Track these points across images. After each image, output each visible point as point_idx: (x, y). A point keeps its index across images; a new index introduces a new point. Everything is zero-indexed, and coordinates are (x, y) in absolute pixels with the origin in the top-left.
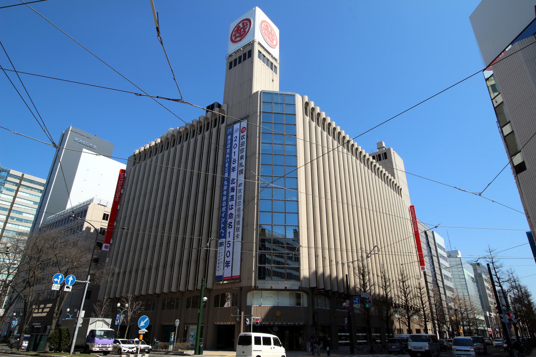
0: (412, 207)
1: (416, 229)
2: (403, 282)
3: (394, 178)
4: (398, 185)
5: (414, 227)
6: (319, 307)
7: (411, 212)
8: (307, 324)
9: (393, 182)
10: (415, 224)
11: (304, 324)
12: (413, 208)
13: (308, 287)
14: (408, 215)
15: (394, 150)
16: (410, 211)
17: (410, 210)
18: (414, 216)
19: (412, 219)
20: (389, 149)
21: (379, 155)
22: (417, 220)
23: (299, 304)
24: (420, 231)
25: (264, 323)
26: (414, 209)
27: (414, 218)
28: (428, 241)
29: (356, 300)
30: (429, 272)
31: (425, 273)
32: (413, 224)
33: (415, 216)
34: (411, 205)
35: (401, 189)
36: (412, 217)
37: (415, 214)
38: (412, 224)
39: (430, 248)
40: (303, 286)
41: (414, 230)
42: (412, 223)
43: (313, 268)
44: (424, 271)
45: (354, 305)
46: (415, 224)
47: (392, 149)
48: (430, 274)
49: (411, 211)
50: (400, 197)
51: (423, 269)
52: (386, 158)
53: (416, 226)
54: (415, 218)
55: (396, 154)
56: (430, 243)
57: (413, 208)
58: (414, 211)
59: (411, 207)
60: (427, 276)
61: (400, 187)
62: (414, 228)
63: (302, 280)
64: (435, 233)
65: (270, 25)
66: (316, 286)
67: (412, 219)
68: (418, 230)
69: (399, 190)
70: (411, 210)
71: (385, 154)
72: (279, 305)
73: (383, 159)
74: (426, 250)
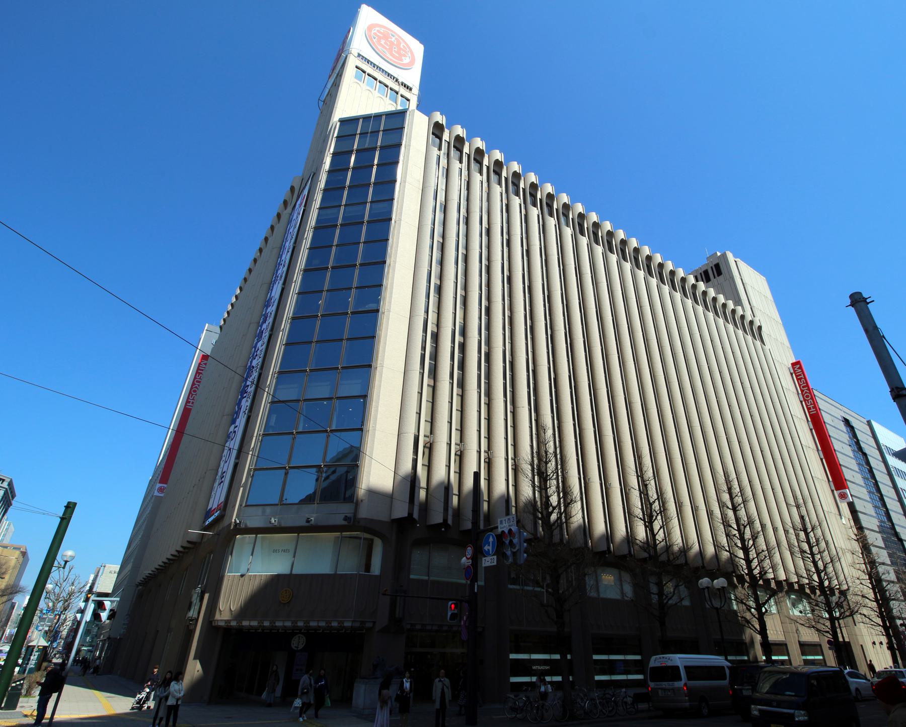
0: (797, 369)
1: (812, 410)
2: (735, 509)
3: (738, 302)
4: (749, 317)
5: (807, 406)
6: (432, 578)
7: (797, 376)
8: (369, 625)
9: (734, 311)
10: (808, 400)
11: (357, 625)
12: (798, 366)
13: (384, 517)
14: (788, 383)
15: (735, 256)
16: (794, 375)
17: (792, 371)
18: (804, 383)
19: (800, 392)
20: (724, 256)
21: (706, 273)
22: (816, 393)
23: (368, 567)
24: (826, 418)
25: (245, 623)
26: (801, 368)
27: (803, 387)
28: (858, 440)
29: (489, 545)
30: (866, 507)
31: (851, 506)
32: (805, 400)
33: (807, 382)
34: (794, 361)
35: (760, 328)
36: (800, 385)
37: (805, 378)
38: (801, 402)
39: (865, 454)
40: (363, 513)
41: (809, 412)
42: (802, 399)
43: (407, 467)
44: (847, 500)
45: (484, 559)
46: (808, 400)
47: (730, 257)
48: (870, 509)
49: (795, 374)
50: (758, 343)
51: (843, 496)
52: (719, 273)
53: (811, 404)
54: (807, 386)
55: (743, 266)
56: (863, 445)
57: (798, 366)
58: (802, 371)
59: (793, 364)
60: (860, 515)
61: (757, 324)
62: (809, 409)
63: (364, 498)
64: (875, 425)
65: (394, 32)
66: (406, 515)
67: (802, 391)
68: (816, 410)
69: (757, 332)
70: (795, 371)
71: (717, 266)
72: (294, 572)
73: (715, 278)
74: (851, 458)
